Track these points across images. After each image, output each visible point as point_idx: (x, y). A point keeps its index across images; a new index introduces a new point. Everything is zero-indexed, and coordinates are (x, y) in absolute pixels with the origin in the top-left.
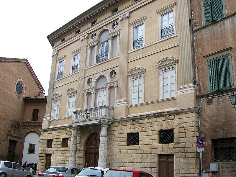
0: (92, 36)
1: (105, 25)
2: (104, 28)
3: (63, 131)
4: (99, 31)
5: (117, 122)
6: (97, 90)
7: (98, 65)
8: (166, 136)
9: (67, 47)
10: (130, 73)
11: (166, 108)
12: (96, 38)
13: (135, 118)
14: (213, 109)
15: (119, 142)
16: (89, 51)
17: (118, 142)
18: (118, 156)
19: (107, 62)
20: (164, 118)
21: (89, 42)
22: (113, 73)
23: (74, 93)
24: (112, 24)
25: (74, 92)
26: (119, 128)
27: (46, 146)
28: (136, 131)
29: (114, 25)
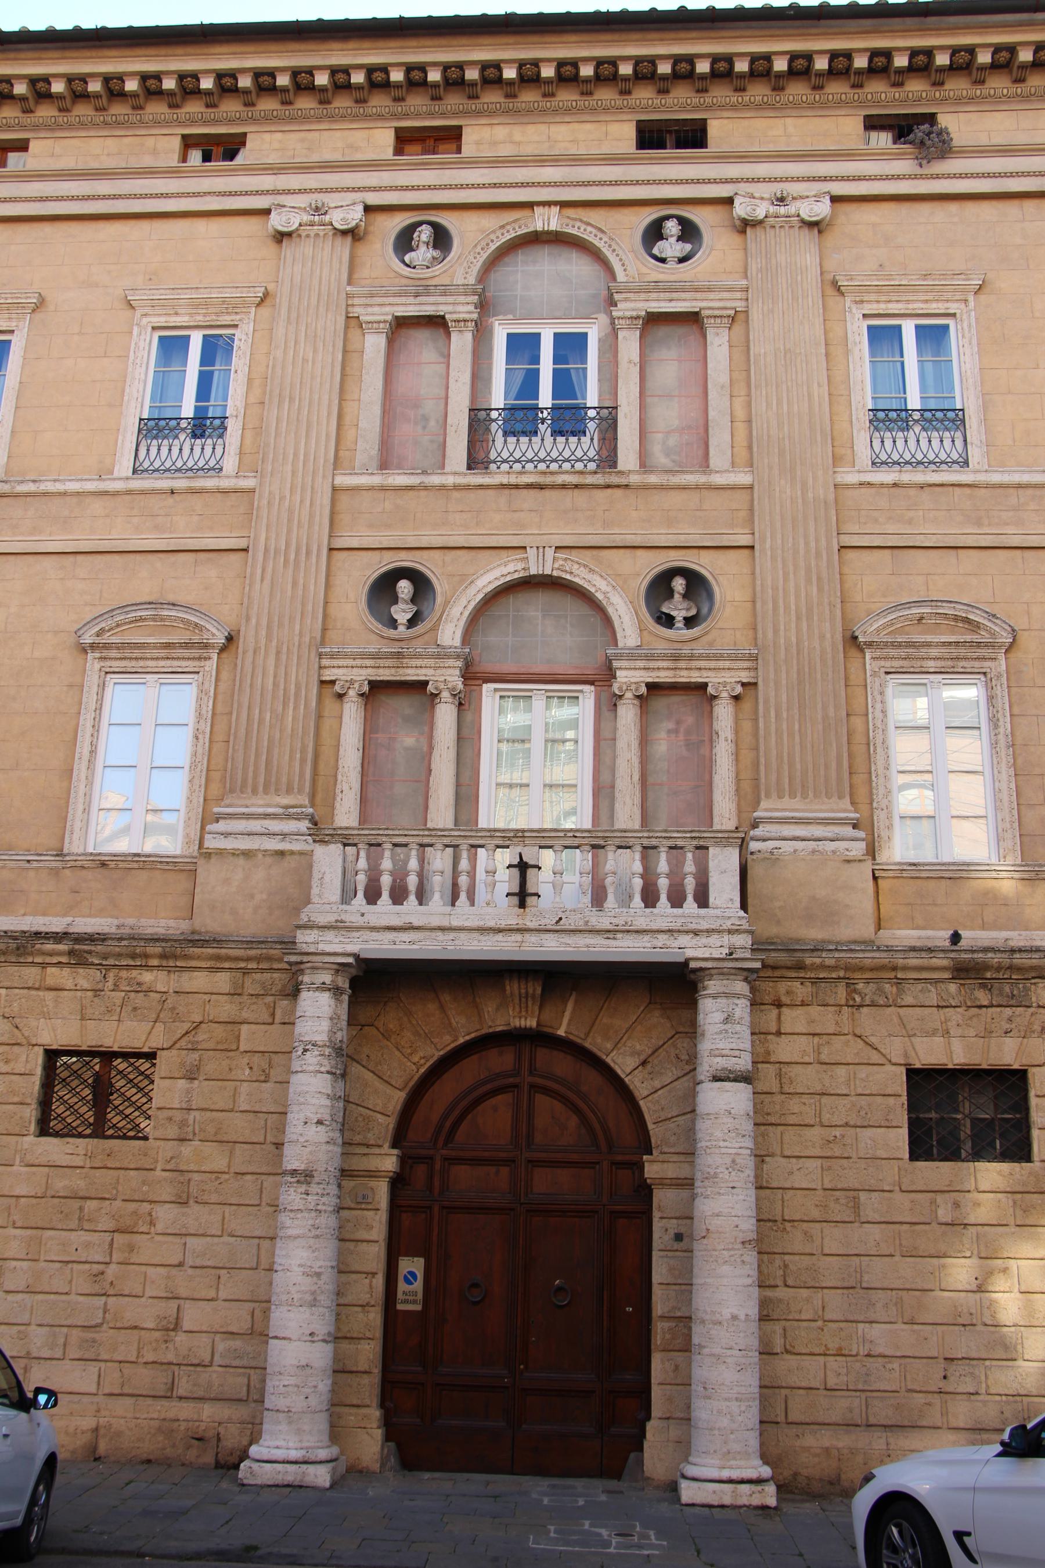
0: (405, 242)
1: (564, 205)
2: (549, 220)
4: (489, 221)
5: (800, 966)
6: (473, 676)
7: (503, 486)
9: (47, 228)
10: (878, 630)
12: (463, 264)
13: (993, 958)
15: (837, 1132)
16: (375, 344)
17: (817, 1131)
18: (833, 1239)
19: (608, 486)
21: (363, 273)
22: (678, 590)
23: (195, 652)
24: (648, 216)
25: (186, 645)
26: (825, 1019)
28: (1006, 1054)
29: (654, 233)
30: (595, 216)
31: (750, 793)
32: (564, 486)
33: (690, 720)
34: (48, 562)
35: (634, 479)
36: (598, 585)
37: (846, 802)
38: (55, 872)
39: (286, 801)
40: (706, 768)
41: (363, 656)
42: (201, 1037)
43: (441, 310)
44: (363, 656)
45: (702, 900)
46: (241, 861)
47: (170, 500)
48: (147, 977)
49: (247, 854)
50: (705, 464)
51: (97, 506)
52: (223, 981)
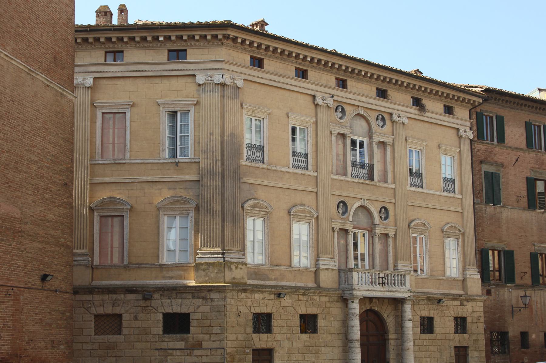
3: (301, 297)
8: (461, 324)
11: (452, 289)
14: (491, 301)
20: (457, 303)
27: (250, 329)
30: (369, 111)
31: (396, 260)
32: (366, 184)
33: (383, 241)
34: (280, 190)
35: (377, 184)
36: (372, 209)
37: (409, 262)
38: (291, 271)
39: (329, 256)
40: (387, 252)
41: (339, 222)
42: (325, 311)
43: (345, 132)
44: (339, 222)
45: (405, 284)
46: (327, 271)
47: (301, 176)
48: (315, 298)
49: (327, 269)
50: (385, 181)
51: (287, 176)
52: (327, 299)
